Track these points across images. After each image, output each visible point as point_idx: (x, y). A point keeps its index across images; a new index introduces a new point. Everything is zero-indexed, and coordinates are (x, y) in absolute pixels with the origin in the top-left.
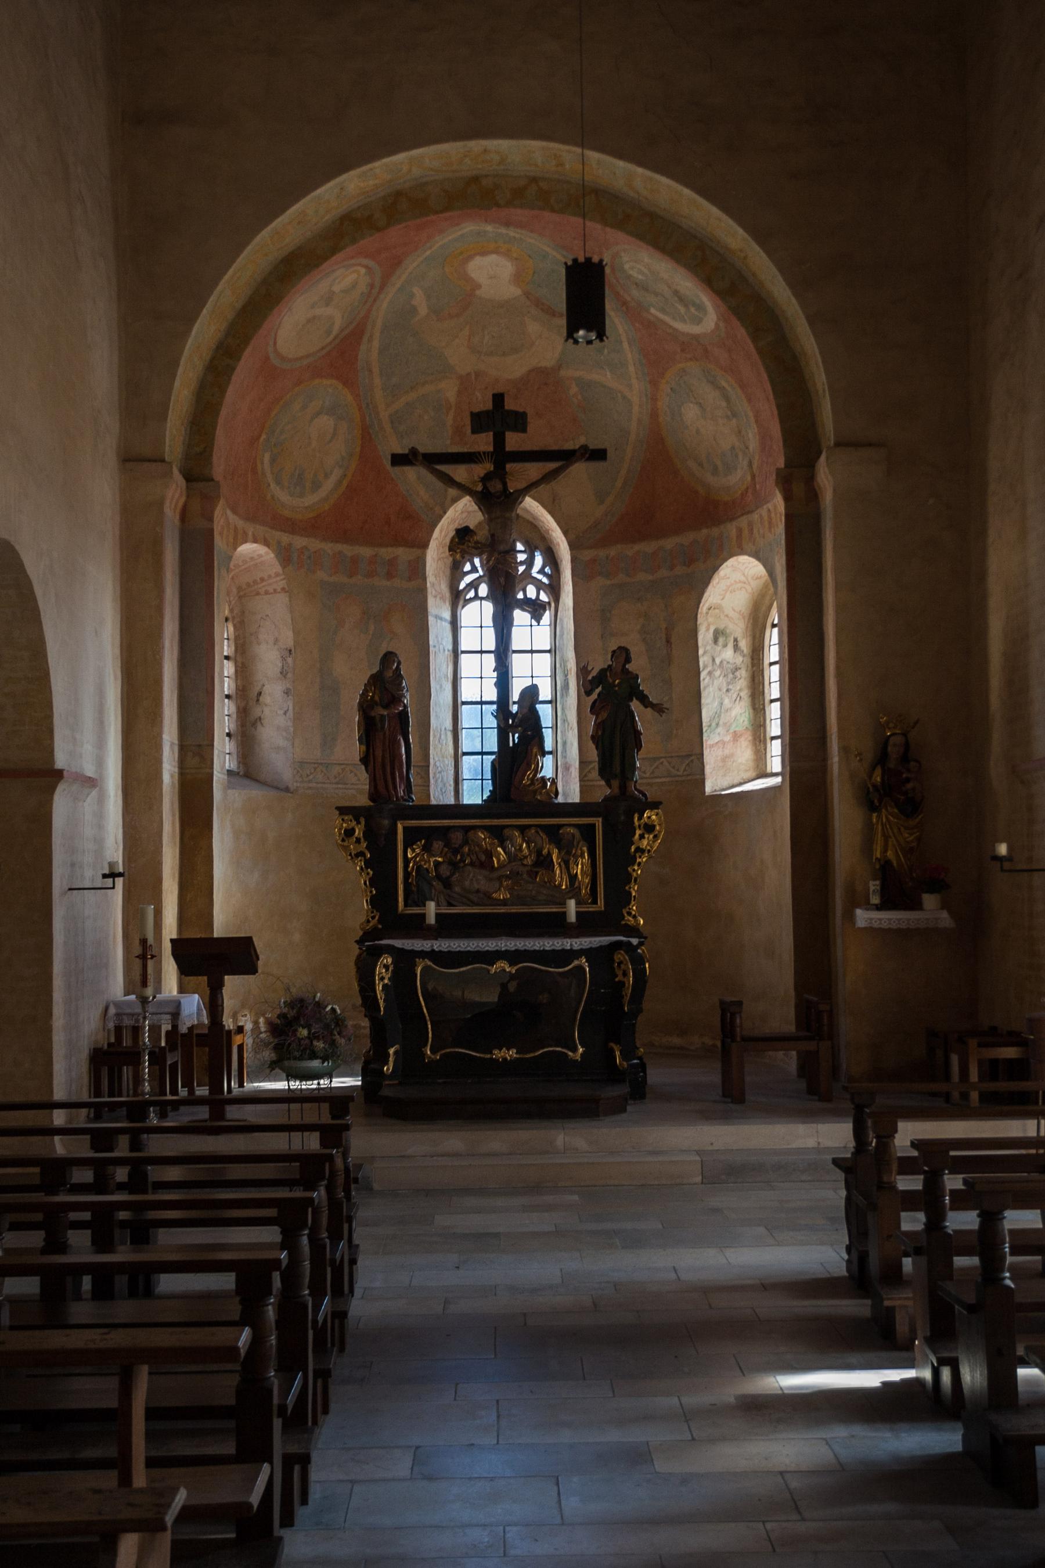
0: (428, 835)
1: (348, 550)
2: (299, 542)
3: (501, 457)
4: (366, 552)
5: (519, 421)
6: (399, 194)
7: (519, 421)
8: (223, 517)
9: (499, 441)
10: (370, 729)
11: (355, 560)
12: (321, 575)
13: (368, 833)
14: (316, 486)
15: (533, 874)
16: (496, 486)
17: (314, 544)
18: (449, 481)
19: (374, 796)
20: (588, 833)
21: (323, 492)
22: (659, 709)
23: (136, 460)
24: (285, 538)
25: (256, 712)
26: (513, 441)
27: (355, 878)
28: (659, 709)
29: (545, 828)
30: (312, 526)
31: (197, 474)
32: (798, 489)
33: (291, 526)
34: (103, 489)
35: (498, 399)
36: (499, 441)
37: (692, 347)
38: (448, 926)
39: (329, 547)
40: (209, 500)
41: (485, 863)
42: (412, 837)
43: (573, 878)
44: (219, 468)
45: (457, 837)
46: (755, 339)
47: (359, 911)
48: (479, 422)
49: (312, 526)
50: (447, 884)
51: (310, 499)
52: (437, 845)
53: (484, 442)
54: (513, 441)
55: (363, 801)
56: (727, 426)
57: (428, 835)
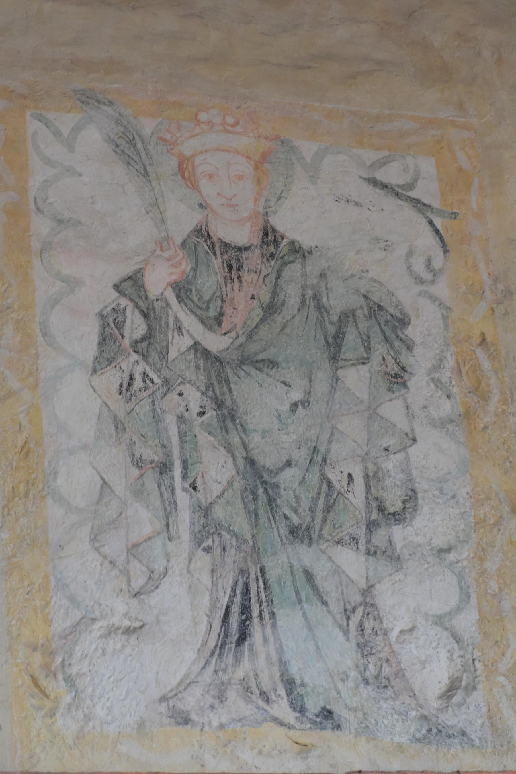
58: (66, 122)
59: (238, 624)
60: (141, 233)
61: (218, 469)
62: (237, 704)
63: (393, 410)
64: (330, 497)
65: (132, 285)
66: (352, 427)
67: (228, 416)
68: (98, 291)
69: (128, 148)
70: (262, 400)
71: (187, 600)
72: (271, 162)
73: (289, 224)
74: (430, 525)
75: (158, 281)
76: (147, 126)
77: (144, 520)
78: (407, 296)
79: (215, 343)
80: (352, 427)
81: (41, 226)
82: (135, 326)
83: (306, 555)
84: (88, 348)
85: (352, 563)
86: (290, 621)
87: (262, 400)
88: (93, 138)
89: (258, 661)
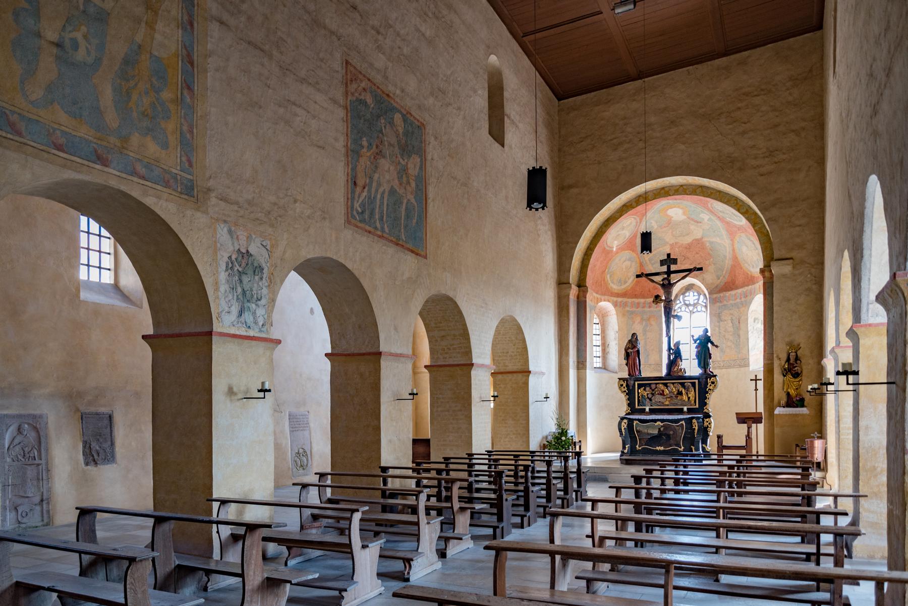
0: (645, 385)
1: (636, 300)
2: (620, 299)
3: (669, 272)
4: (642, 300)
5: (675, 261)
6: (640, 196)
7: (675, 261)
8: (590, 297)
9: (669, 267)
10: (627, 356)
11: (638, 303)
12: (628, 309)
13: (627, 385)
14: (625, 282)
15: (677, 397)
16: (666, 282)
17: (625, 300)
18: (653, 281)
19: (629, 375)
20: (693, 384)
21: (627, 284)
22: (717, 346)
23: (562, 283)
24: (615, 299)
25: (607, 350)
26: (673, 268)
27: (622, 399)
28: (717, 346)
29: (681, 383)
30: (624, 295)
31: (581, 285)
32: (767, 274)
33: (618, 295)
34: (549, 294)
35: (669, 255)
36: (669, 267)
37: (740, 228)
38: (652, 411)
39: (630, 300)
40: (586, 292)
41: (662, 394)
42: (640, 386)
43: (689, 398)
44: (589, 282)
45: (653, 386)
46: (754, 227)
47: (623, 409)
48: (662, 263)
49: (624, 295)
50: (650, 400)
51: (623, 287)
52: (648, 389)
53: (664, 269)
54: (673, 268)
55: (627, 376)
56: (751, 255)
57: (645, 385)
58: (222, 226)
59: (241, 313)
60: (231, 248)
61: (239, 290)
62: (240, 325)
63: (260, 284)
64: (252, 296)
65: (230, 257)
66: (255, 285)
67: (241, 281)
68: (226, 259)
69: (230, 232)
70: (245, 279)
71: (235, 310)
72: (249, 238)
73: (250, 250)
74: (263, 302)
75: (233, 257)
76: (233, 229)
77: (231, 297)
78: (264, 265)
79: (240, 269)
80: (255, 285)
81: (219, 245)
82: (230, 265)
83: (249, 304)
84: (224, 268)
85: (254, 306)
86: (246, 313)
87: (245, 279)
88: (225, 229)
89: (242, 319)
